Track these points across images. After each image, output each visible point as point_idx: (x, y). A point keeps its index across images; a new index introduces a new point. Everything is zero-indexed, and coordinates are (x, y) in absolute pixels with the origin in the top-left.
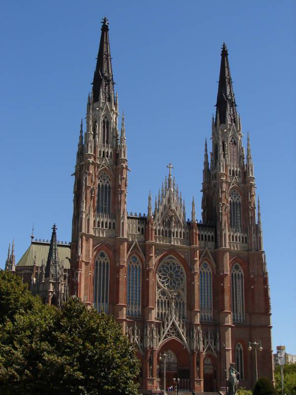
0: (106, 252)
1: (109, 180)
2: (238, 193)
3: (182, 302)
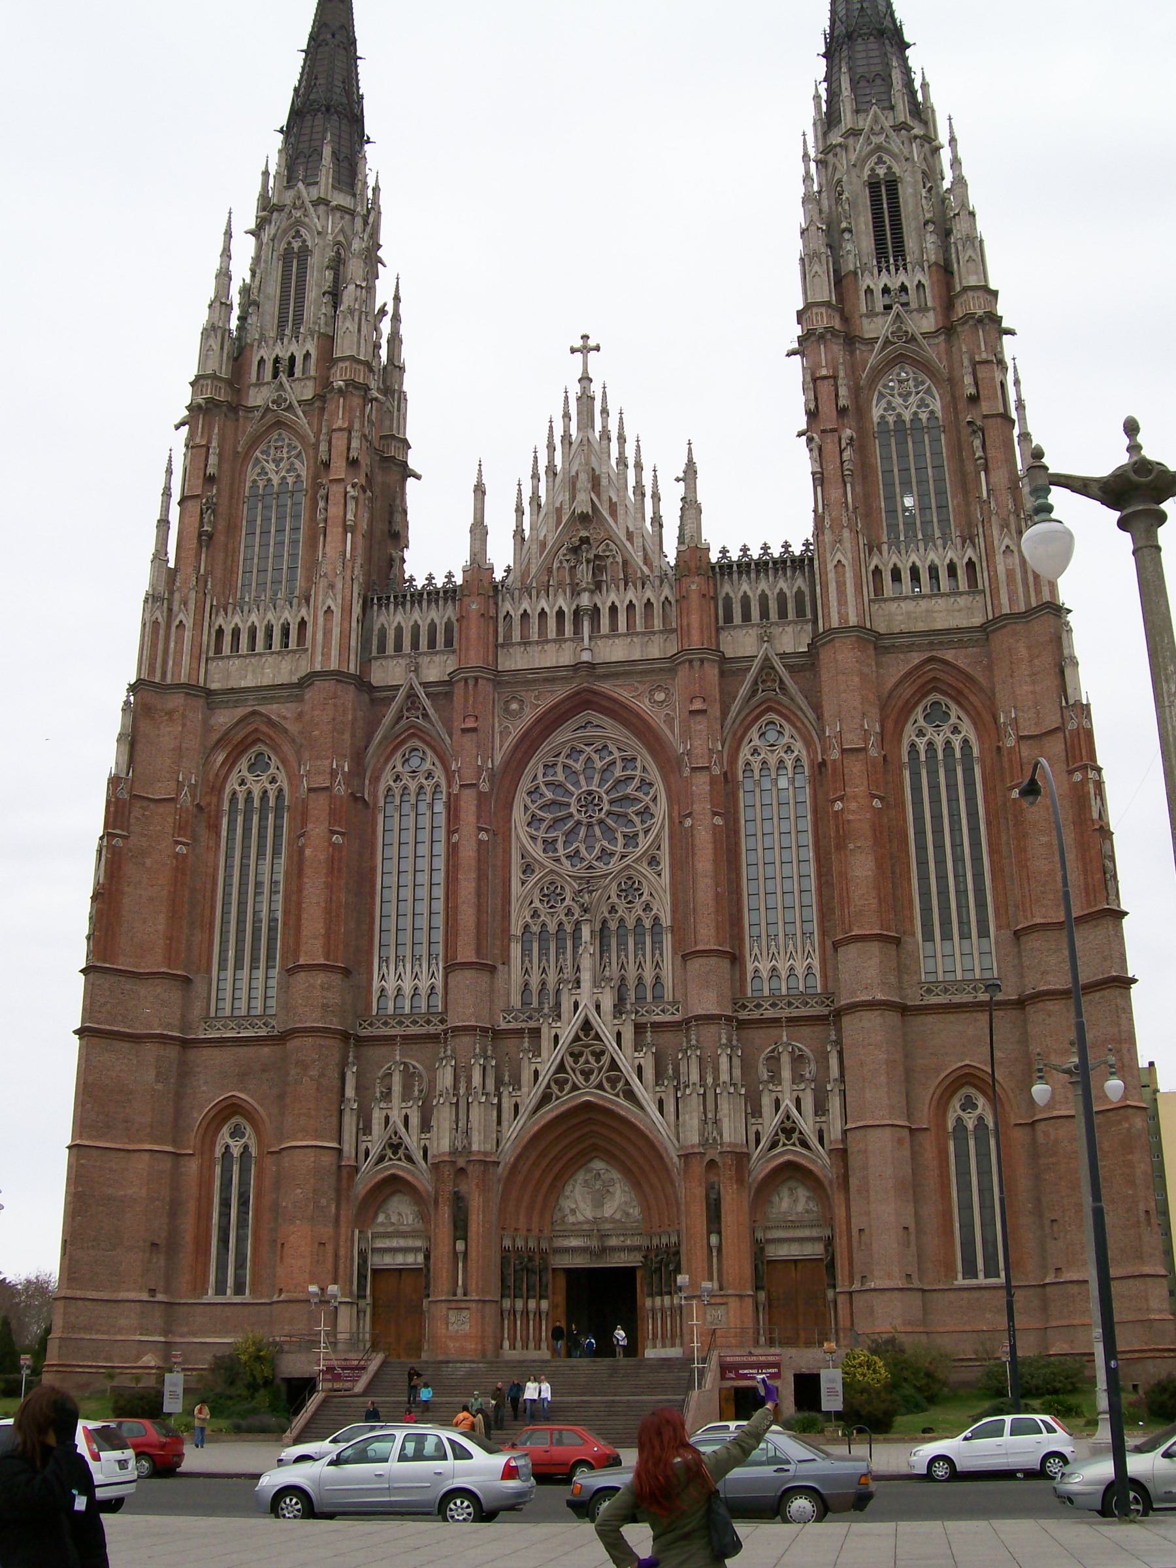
2: (922, 377)
3: (647, 923)
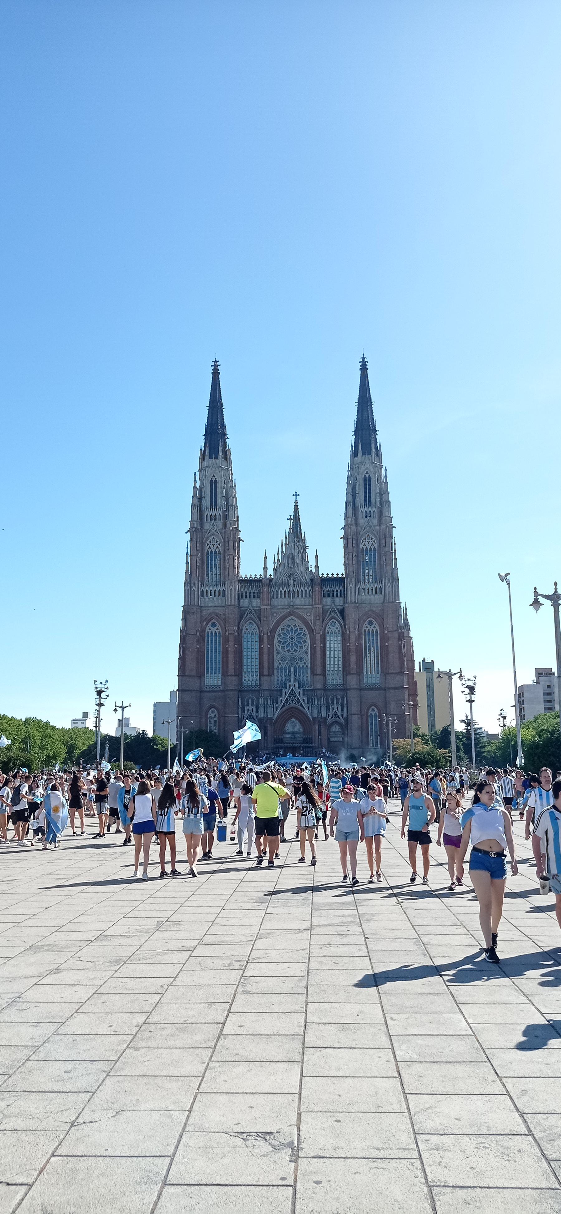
0: (217, 621)
1: (219, 544)
